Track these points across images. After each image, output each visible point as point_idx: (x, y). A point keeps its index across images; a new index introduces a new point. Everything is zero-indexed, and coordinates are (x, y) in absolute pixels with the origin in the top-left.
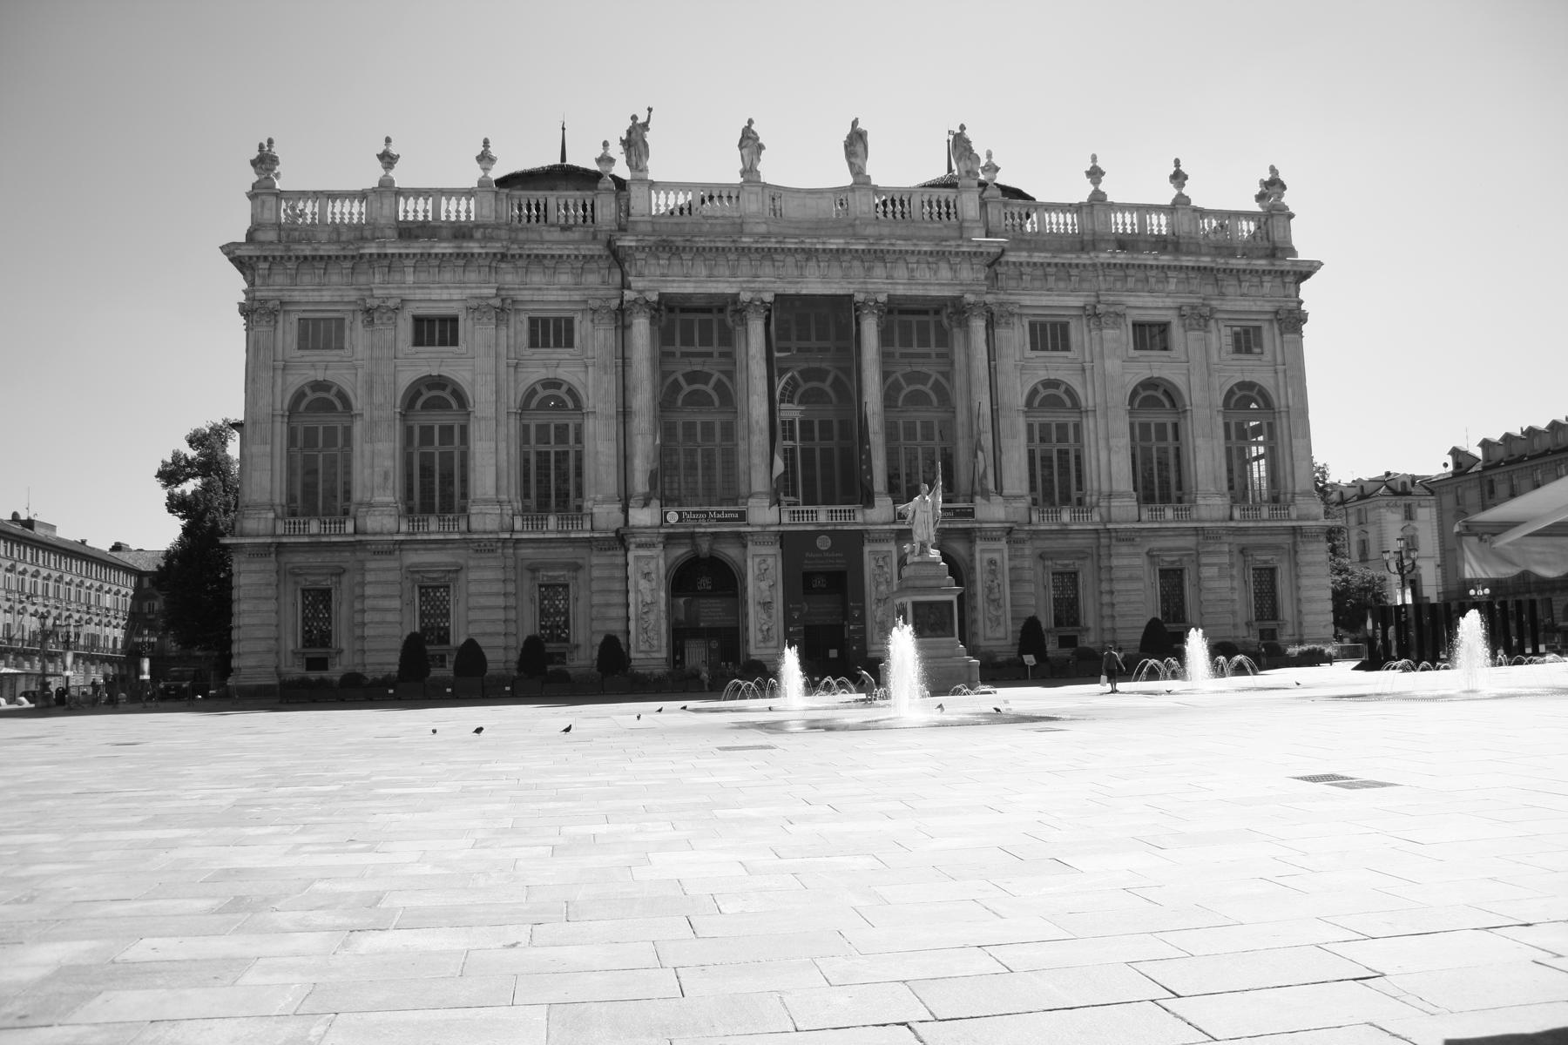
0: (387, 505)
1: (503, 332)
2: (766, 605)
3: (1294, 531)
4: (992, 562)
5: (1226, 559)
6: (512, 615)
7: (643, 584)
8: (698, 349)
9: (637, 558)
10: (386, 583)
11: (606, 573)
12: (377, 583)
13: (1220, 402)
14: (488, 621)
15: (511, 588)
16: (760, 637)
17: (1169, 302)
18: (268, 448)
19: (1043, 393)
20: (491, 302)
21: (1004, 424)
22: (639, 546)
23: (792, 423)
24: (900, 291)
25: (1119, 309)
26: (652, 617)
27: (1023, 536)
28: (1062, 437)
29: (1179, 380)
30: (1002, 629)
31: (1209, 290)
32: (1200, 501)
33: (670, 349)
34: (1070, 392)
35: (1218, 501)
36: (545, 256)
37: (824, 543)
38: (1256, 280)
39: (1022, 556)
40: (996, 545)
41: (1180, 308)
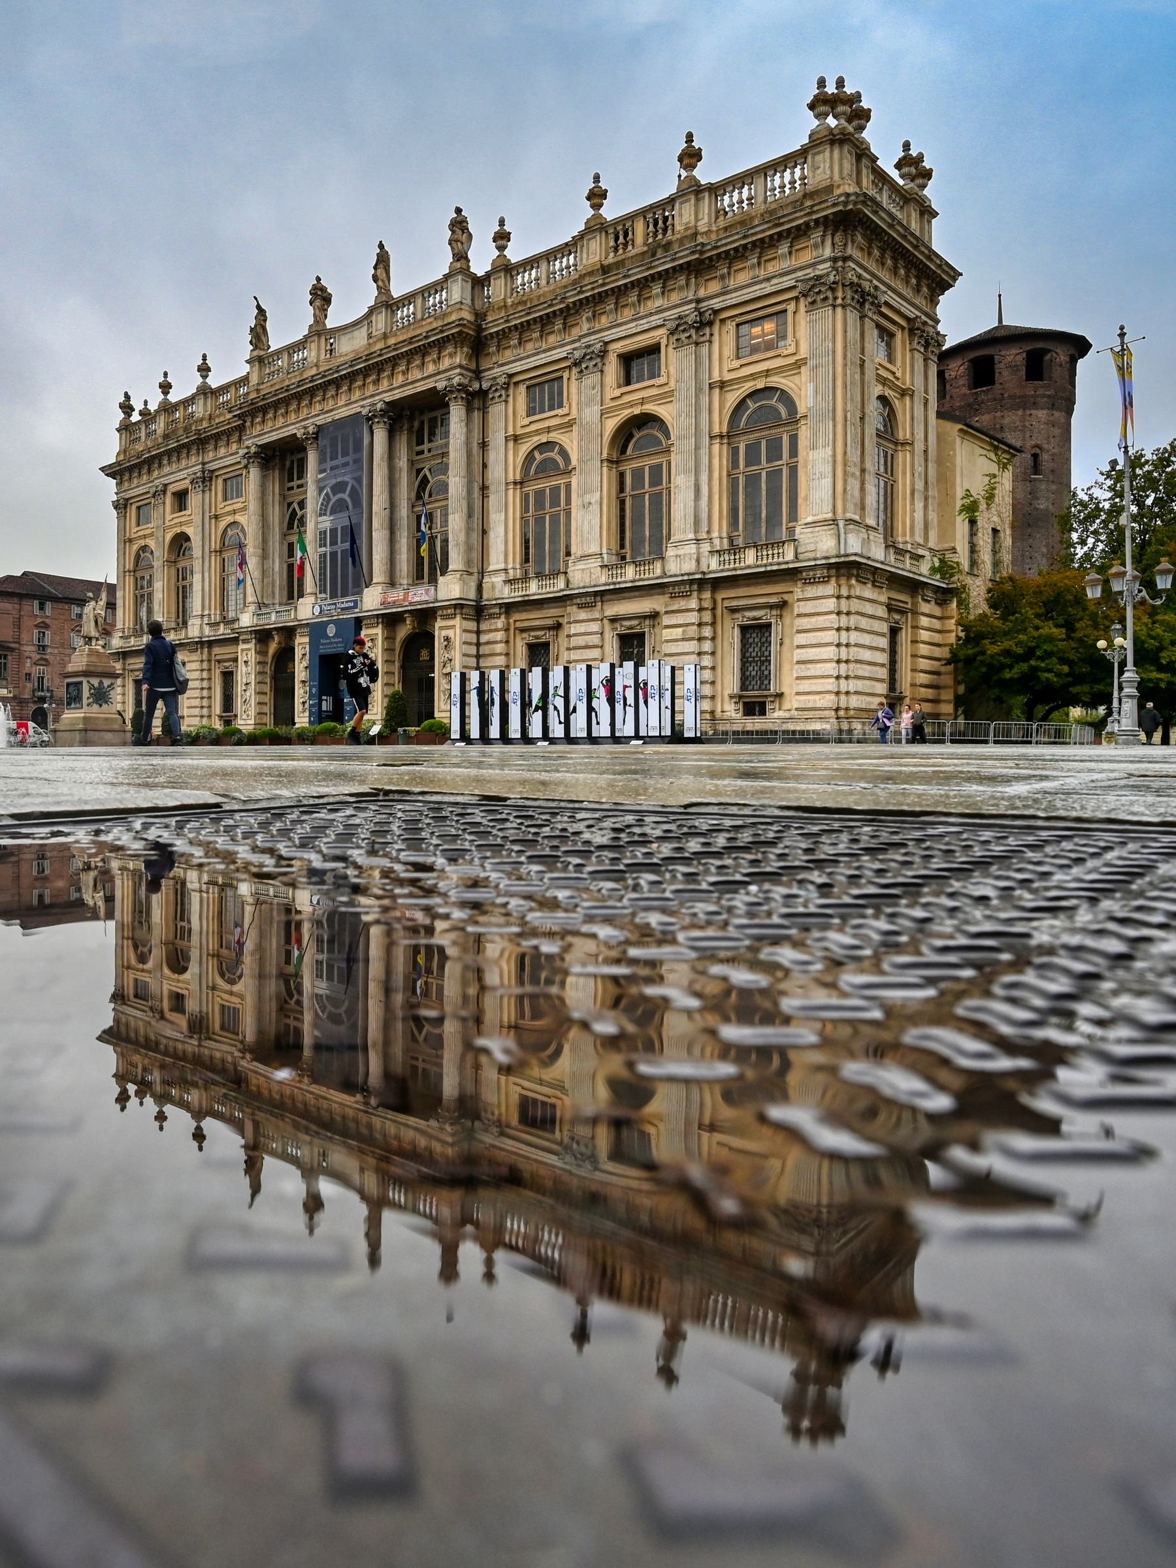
1: (207, 495)
3: (791, 574)
4: (447, 639)
5: (693, 617)
6: (205, 693)
7: (244, 668)
9: (243, 650)
13: (720, 426)
15: (205, 675)
17: (656, 320)
21: (493, 500)
23: (325, 532)
26: (248, 693)
27: (497, 610)
28: (555, 502)
29: (662, 411)
31: (714, 287)
32: (670, 552)
33: (291, 484)
34: (564, 453)
35: (692, 549)
37: (331, 631)
38: (770, 254)
39: (497, 630)
40: (450, 623)
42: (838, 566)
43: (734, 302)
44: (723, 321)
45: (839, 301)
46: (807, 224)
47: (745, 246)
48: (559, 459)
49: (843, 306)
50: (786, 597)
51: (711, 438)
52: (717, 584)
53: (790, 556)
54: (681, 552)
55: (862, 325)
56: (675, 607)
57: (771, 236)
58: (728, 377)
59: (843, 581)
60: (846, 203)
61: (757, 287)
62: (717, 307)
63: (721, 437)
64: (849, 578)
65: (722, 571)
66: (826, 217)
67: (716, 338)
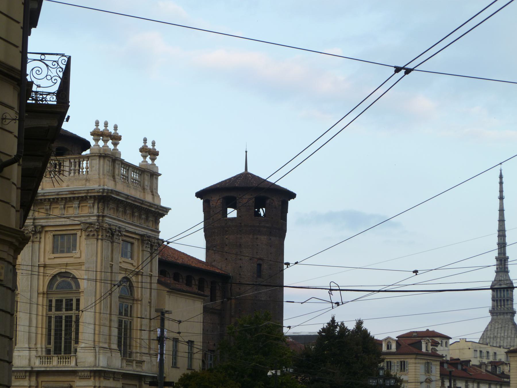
3: (73, 373)
35: (26, 353)
42: (95, 372)
43: (52, 224)
44: (46, 231)
45: (100, 237)
46: (86, 197)
47: (58, 199)
49: (102, 240)
50: (72, 383)
51: (38, 293)
52: (39, 373)
53: (73, 364)
54: (21, 354)
55: (112, 246)
57: (70, 198)
58: (48, 262)
59: (97, 378)
60: (103, 192)
61: (63, 220)
62: (44, 224)
63: (44, 293)
64: (100, 377)
65: (41, 367)
66: (94, 196)
67: (43, 240)
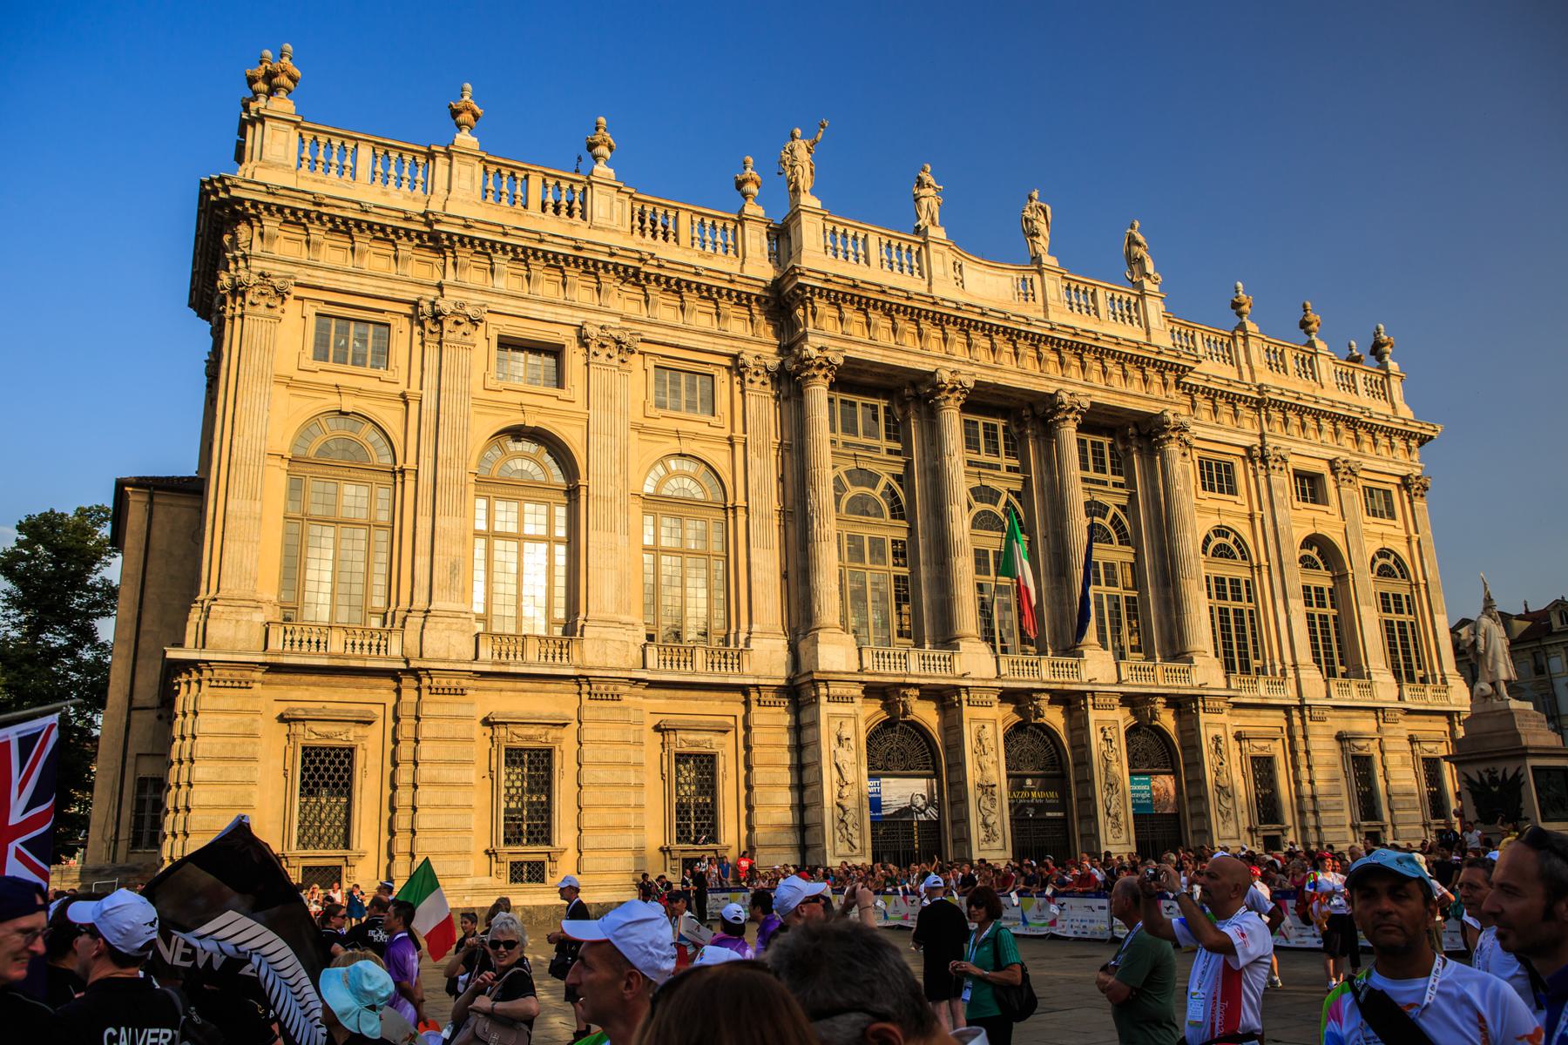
0: (456, 615)
2: (986, 788)
8: (861, 439)
9: (832, 716)
10: (453, 739)
11: (772, 740)
12: (436, 739)
14: (610, 806)
16: (983, 834)
18: (258, 504)
19: (1216, 541)
20: (615, 334)
22: (832, 699)
24: (1100, 398)
25: (1282, 452)
29: (1339, 540)
30: (1232, 825)
36: (689, 284)
41: (1331, 462)
48: (1234, 548)
56: (1391, 733)
